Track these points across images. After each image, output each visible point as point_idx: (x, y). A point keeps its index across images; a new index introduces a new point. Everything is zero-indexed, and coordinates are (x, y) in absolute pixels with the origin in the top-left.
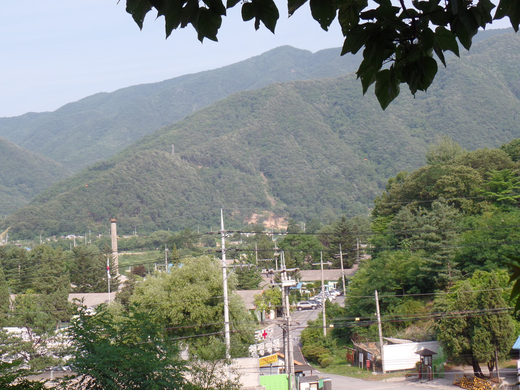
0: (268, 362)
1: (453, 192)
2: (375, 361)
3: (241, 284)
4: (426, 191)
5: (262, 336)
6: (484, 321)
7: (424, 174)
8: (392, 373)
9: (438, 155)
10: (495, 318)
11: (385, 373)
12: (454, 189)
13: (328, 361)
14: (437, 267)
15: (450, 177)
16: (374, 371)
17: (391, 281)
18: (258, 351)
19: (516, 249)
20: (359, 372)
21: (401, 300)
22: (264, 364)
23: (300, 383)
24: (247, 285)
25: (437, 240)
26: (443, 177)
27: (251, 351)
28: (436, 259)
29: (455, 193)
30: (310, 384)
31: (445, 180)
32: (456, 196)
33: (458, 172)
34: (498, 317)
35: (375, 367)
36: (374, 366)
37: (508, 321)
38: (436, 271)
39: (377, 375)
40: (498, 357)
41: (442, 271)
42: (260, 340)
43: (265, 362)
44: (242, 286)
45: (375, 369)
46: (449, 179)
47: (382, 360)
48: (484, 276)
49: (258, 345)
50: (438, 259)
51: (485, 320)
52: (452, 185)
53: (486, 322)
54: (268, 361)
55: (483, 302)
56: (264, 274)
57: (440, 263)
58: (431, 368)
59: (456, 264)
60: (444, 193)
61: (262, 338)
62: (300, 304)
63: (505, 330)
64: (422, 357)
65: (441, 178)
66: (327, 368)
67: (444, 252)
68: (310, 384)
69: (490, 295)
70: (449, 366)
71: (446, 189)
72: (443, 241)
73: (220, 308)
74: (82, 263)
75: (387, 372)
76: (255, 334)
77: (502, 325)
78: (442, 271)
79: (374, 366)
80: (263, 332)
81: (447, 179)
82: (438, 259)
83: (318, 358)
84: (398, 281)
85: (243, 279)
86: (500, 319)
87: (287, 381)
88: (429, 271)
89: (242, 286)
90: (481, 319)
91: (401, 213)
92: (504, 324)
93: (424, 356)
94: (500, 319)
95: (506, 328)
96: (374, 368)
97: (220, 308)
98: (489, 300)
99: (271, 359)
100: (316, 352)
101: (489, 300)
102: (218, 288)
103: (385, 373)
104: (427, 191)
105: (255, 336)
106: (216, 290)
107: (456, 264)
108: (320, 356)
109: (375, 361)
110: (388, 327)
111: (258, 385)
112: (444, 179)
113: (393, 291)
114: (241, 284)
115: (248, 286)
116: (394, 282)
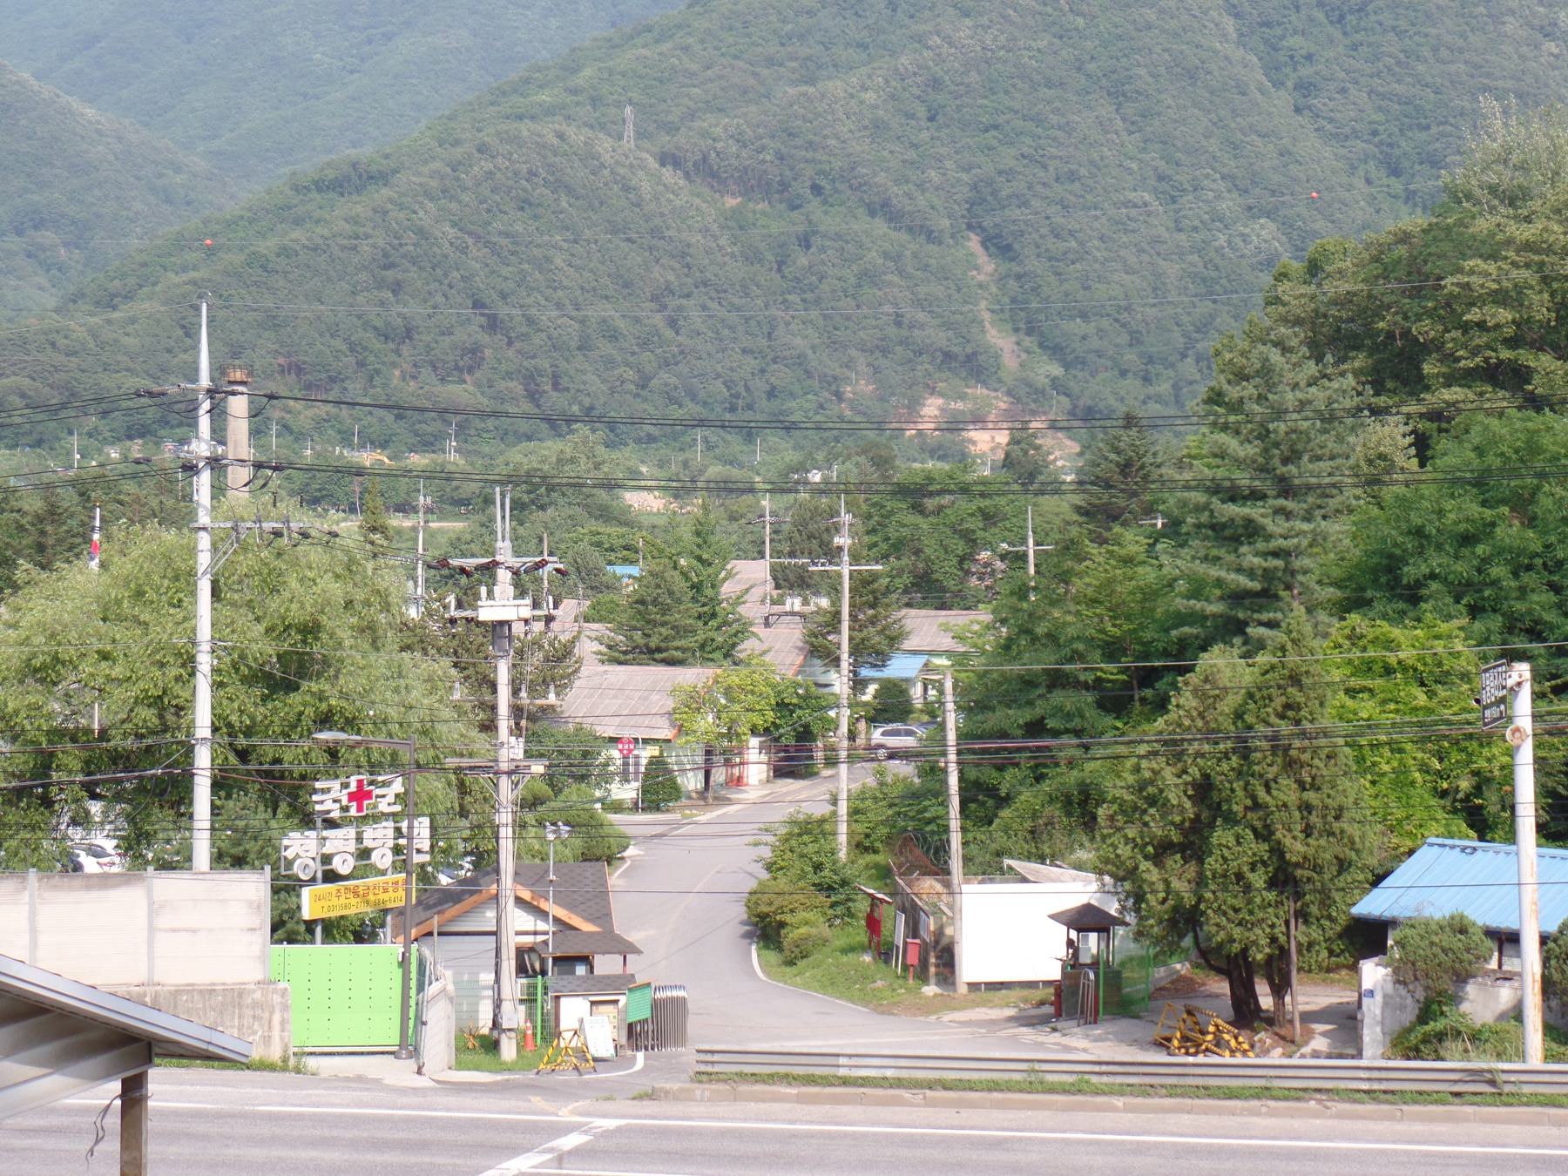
0: (368, 902)
1: (1498, 326)
2: (937, 942)
3: (654, 642)
4: (1399, 318)
5: (345, 802)
6: (1249, 802)
7: (1402, 251)
8: (991, 994)
9: (1491, 178)
10: (1287, 791)
11: (963, 989)
12: (1505, 315)
13: (806, 939)
14: (1247, 602)
15: (1491, 267)
16: (933, 980)
17: (1080, 646)
18: (327, 859)
19: (1547, 547)
20: (879, 984)
21: (1119, 725)
22: (345, 907)
23: (558, 998)
24: (677, 649)
25: (1256, 496)
26: (1469, 264)
27: (289, 854)
28: (1239, 570)
29: (1509, 331)
30: (593, 1003)
31: (1473, 279)
32: (1513, 343)
33: (1528, 246)
34: (1302, 786)
35: (937, 966)
36: (933, 960)
37: (1341, 809)
38: (1241, 615)
39: (936, 995)
40: (1299, 945)
41: (1265, 616)
42: (335, 814)
43: (353, 901)
44: (659, 650)
45: (937, 974)
46: (1487, 274)
47: (957, 938)
48: (1370, 637)
49: (325, 833)
50: (1251, 574)
51: (1254, 798)
52: (1500, 298)
53: (1256, 805)
54: (371, 897)
55: (1250, 728)
56: (793, 614)
57: (1255, 585)
58: (1092, 976)
59: (1330, 592)
60: (1465, 328)
61: (345, 809)
62: (883, 734)
63: (1323, 842)
64: (1073, 934)
65: (1460, 270)
66: (801, 964)
67: (1275, 544)
68: (593, 1003)
69: (1279, 701)
70: (1199, 976)
71: (1473, 315)
72: (1281, 502)
73: (308, 698)
74: (49, 528)
75: (974, 987)
76: (315, 791)
77: (1314, 819)
78: (1265, 616)
79: (933, 960)
80: (353, 787)
81: (1481, 273)
82: (1251, 574)
83: (782, 925)
84: (1112, 650)
85: (664, 624)
86: (1311, 796)
87: (398, 973)
88: (1214, 616)
89: (659, 650)
90: (1240, 793)
91: (1195, 386)
92: (1324, 817)
93: (1079, 930)
94: (1311, 796)
95: (1331, 834)
96: (932, 970)
97: (308, 698)
98: (1273, 719)
99: (386, 890)
100: (778, 902)
101: (1273, 719)
102: (306, 626)
103: (963, 989)
104: (1406, 318)
105: (315, 798)
106: (299, 631)
107: (1330, 592)
108: (788, 918)
109: (937, 942)
110: (1050, 823)
111: (259, 976)
112: (1472, 272)
113: (1086, 686)
114: (653, 645)
115: (678, 654)
116: (1097, 654)
